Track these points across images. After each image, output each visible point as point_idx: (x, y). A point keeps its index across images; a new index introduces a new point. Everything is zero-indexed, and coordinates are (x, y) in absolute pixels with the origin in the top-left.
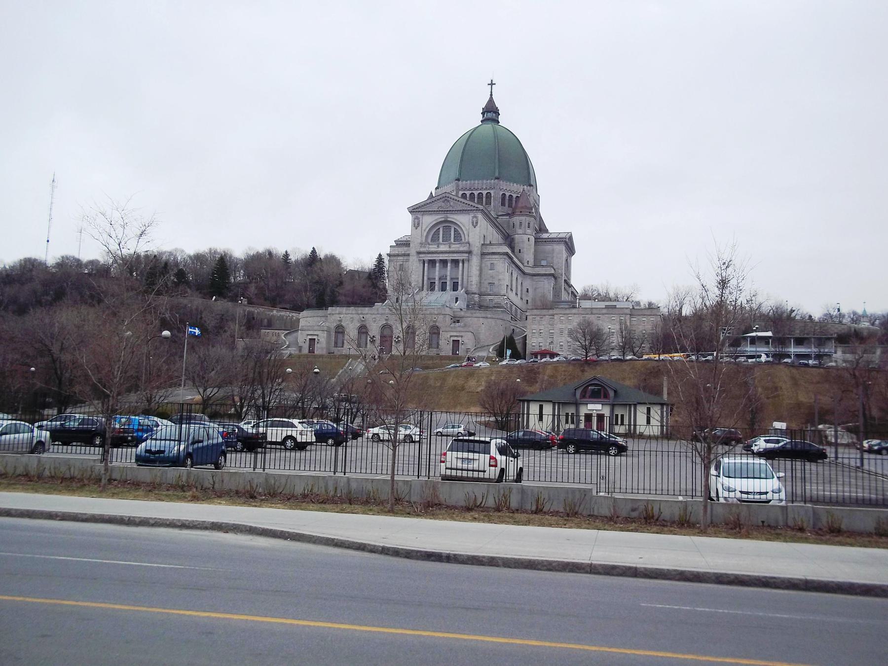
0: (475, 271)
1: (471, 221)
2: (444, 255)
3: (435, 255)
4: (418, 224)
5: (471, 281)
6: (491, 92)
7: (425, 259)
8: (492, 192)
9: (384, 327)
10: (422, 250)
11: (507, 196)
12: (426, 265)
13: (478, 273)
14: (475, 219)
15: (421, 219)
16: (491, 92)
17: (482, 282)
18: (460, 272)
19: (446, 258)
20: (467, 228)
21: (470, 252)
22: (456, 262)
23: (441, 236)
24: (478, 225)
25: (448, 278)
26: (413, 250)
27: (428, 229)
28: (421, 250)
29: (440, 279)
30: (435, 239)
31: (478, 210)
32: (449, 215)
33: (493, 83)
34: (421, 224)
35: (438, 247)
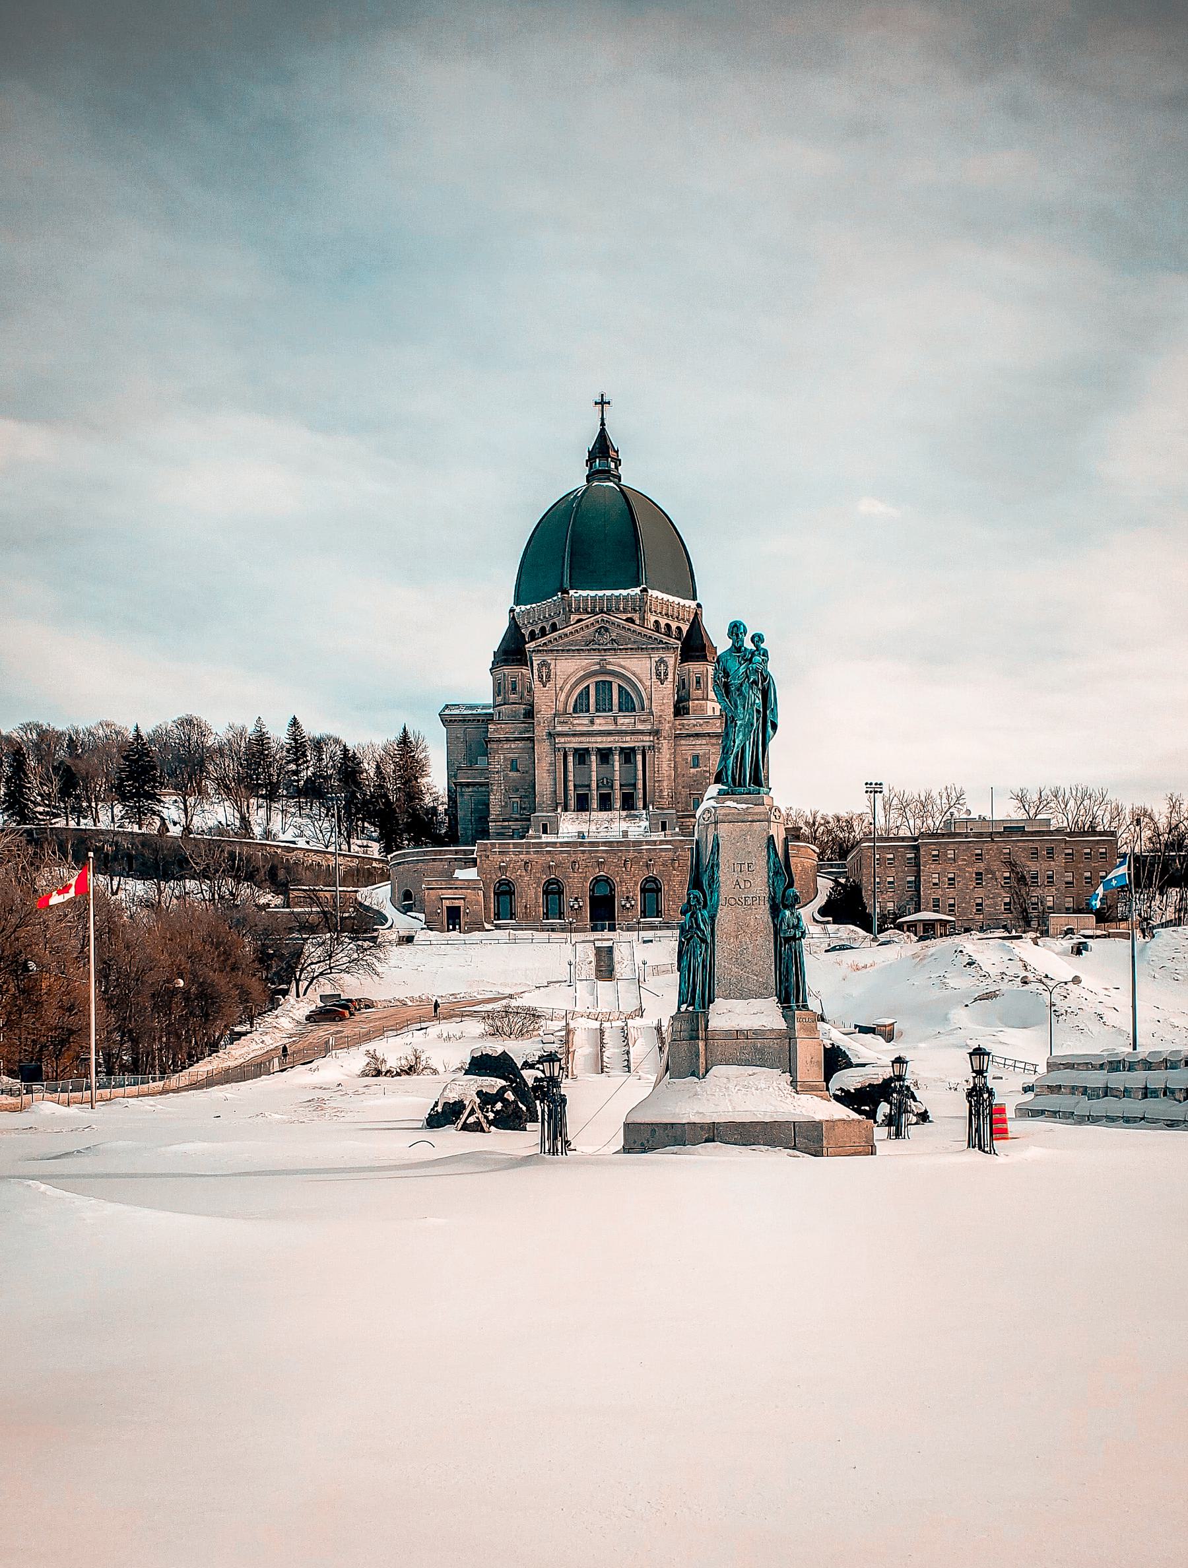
1: (654, 670)
2: (604, 739)
4: (548, 676)
6: (602, 419)
8: (636, 617)
9: (597, 880)
11: (663, 626)
12: (570, 759)
15: (552, 667)
16: (602, 419)
18: (640, 773)
22: (628, 755)
23: (592, 700)
24: (668, 680)
25: (617, 785)
26: (540, 732)
27: (568, 686)
28: (559, 729)
29: (598, 787)
30: (581, 705)
31: (668, 648)
33: (606, 399)
35: (592, 722)
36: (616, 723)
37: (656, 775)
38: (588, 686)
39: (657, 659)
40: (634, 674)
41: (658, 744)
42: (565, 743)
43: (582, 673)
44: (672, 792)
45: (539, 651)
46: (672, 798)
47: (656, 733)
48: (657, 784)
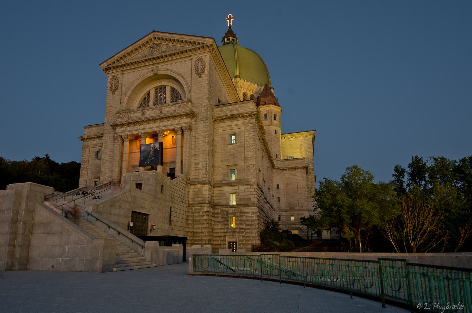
0: (202, 145)
3: (138, 127)
5: (197, 164)
7: (123, 135)
10: (119, 121)
13: (207, 148)
14: (200, 65)
17: (216, 164)
19: (155, 130)
20: (188, 80)
21: (192, 115)
24: (205, 73)
27: (130, 91)
32: (160, 66)
34: (120, 86)
35: (143, 114)
36: (161, 112)
37: (193, 151)
38: (149, 91)
39: (196, 59)
40: (178, 74)
41: (196, 125)
42: (122, 132)
43: (140, 80)
44: (206, 164)
45: (110, 69)
46: (206, 169)
47: (192, 115)
48: (193, 158)
